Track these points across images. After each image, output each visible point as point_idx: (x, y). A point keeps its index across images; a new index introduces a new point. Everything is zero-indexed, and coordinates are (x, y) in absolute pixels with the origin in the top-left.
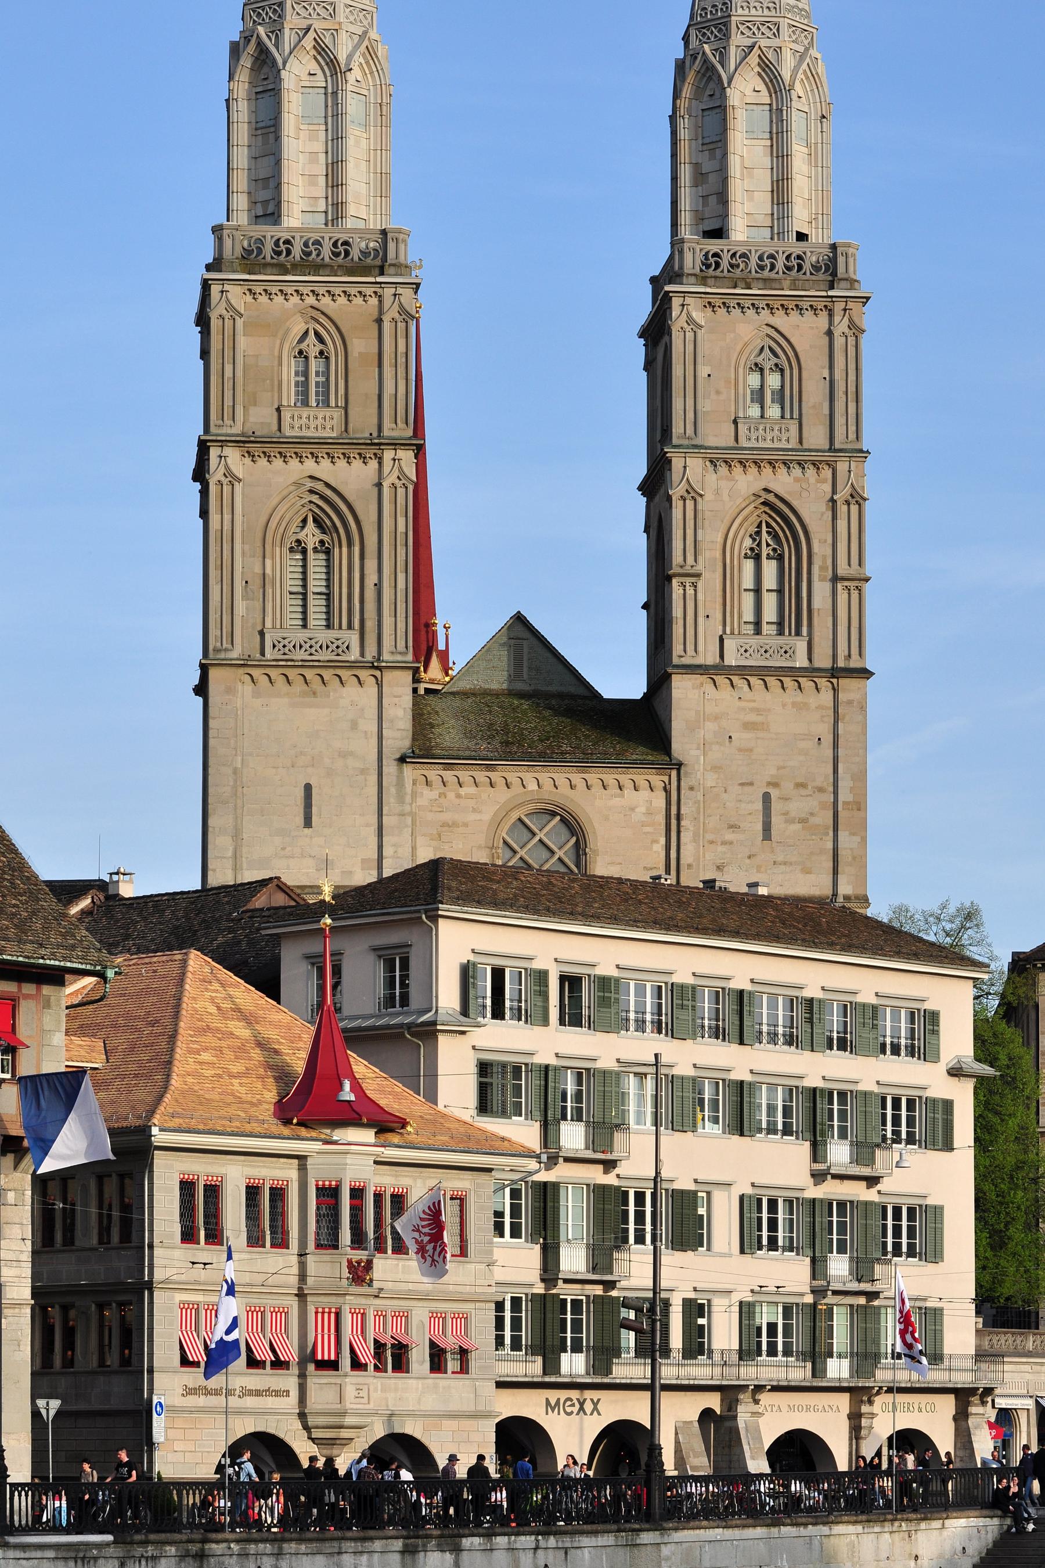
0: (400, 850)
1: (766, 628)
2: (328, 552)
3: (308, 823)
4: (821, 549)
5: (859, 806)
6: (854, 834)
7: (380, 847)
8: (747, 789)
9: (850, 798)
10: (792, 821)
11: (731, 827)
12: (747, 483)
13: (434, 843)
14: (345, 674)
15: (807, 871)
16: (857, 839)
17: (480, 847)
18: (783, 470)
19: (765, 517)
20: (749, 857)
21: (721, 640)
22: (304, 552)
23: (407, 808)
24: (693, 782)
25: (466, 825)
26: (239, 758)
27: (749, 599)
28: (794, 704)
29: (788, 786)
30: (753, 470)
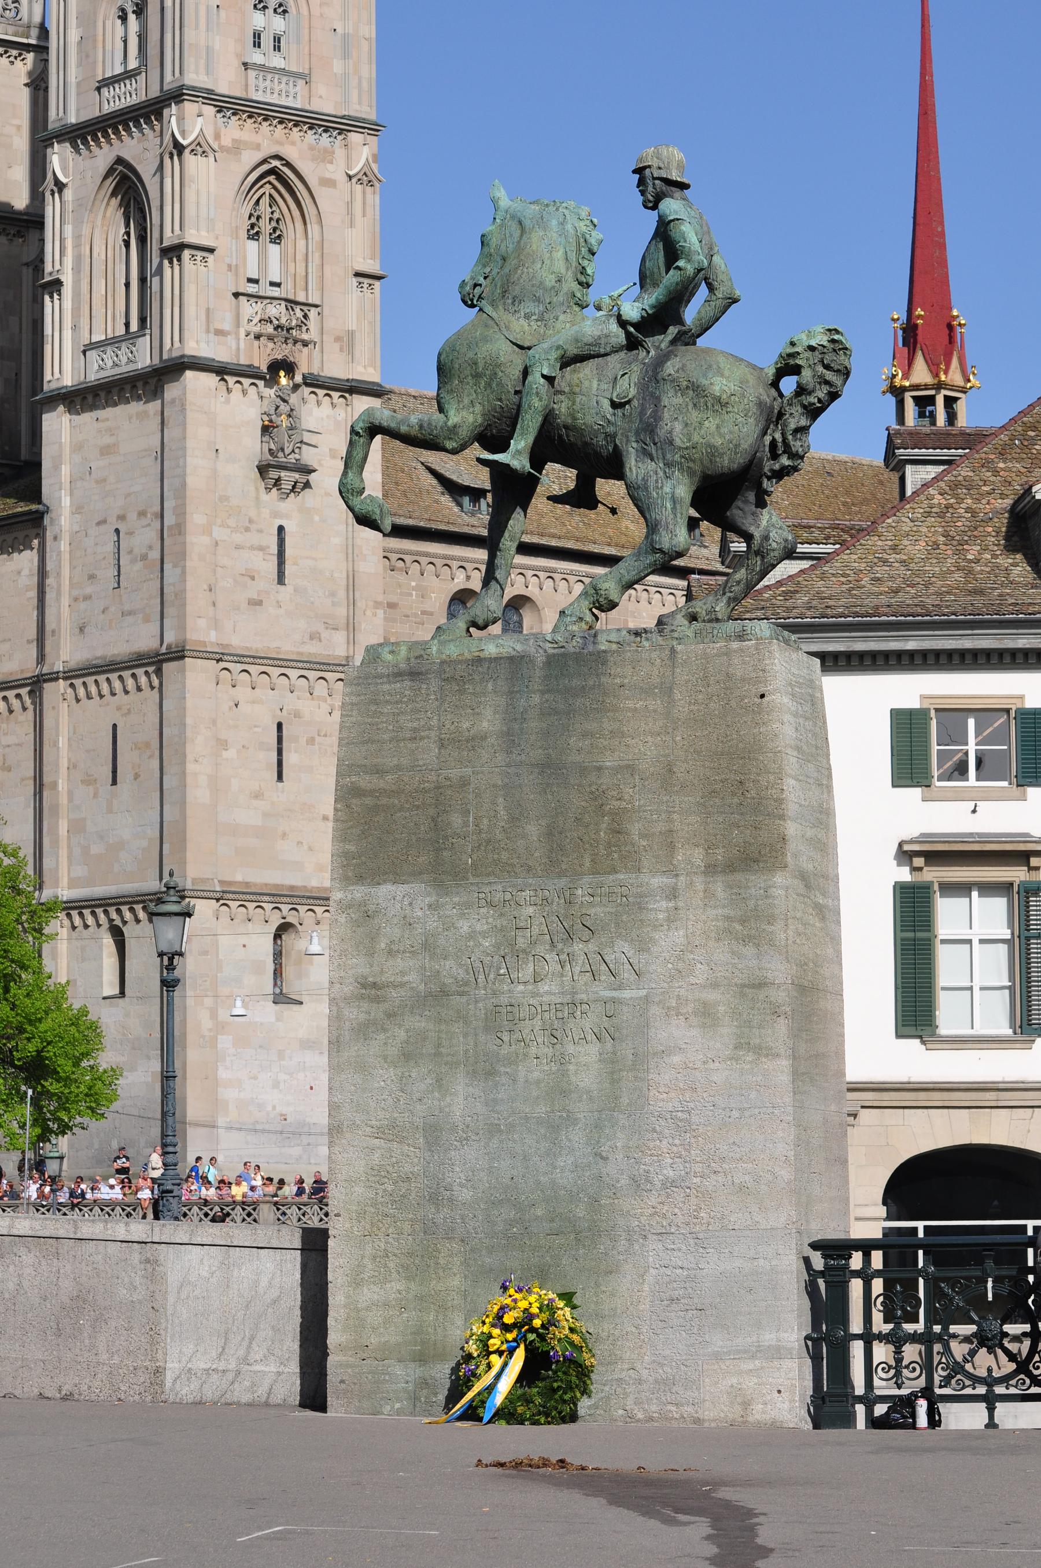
5: (180, 529)
6: (175, 566)
8: (103, 528)
9: (173, 522)
11: (92, 577)
12: (103, 156)
16: (178, 571)
29: (132, 516)
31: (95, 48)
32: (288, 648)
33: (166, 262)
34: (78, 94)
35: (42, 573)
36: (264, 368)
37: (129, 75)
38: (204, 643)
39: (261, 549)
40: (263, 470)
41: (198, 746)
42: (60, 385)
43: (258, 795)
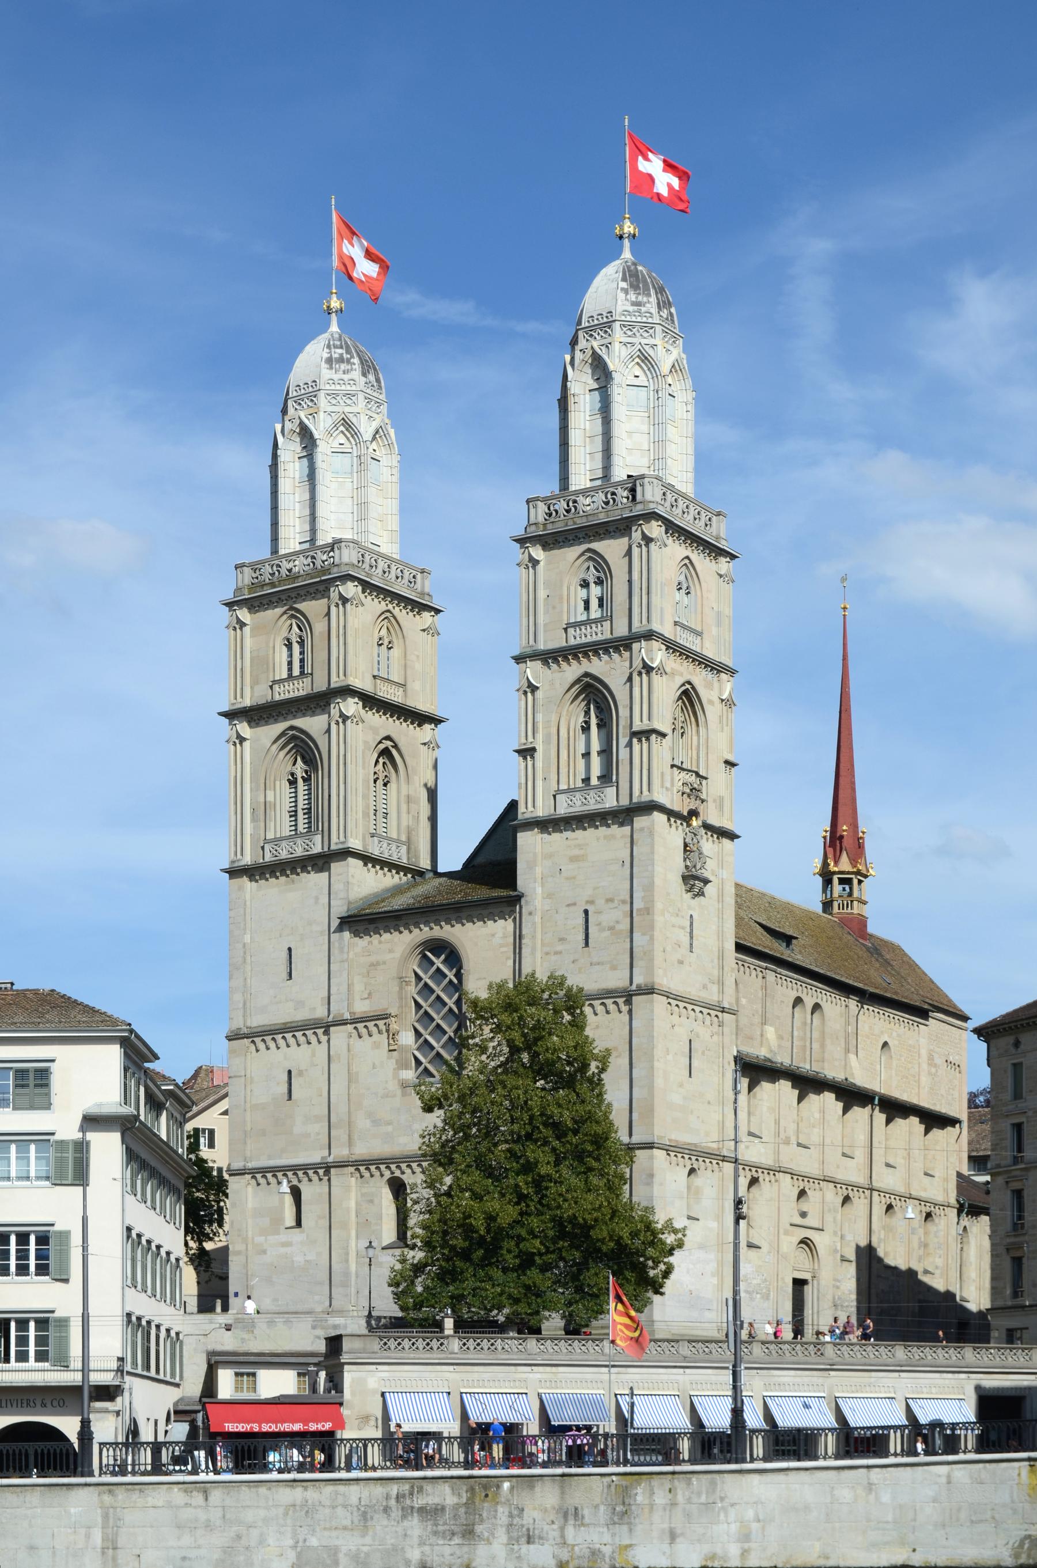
1: (594, 781)
4: (624, 712)
5: (648, 911)
6: (644, 934)
8: (572, 908)
10: (604, 930)
15: (614, 968)
16: (647, 938)
18: (594, 659)
19: (591, 695)
21: (554, 796)
24: (531, 908)
27: (581, 763)
28: (605, 837)
29: (600, 902)
30: (574, 662)
31: (562, 602)
32: (694, 993)
33: (635, 740)
34: (545, 631)
35: (518, 938)
36: (685, 814)
37: (588, 622)
38: (660, 985)
39: (683, 928)
40: (685, 878)
41: (658, 1052)
42: (534, 815)
43: (681, 1085)
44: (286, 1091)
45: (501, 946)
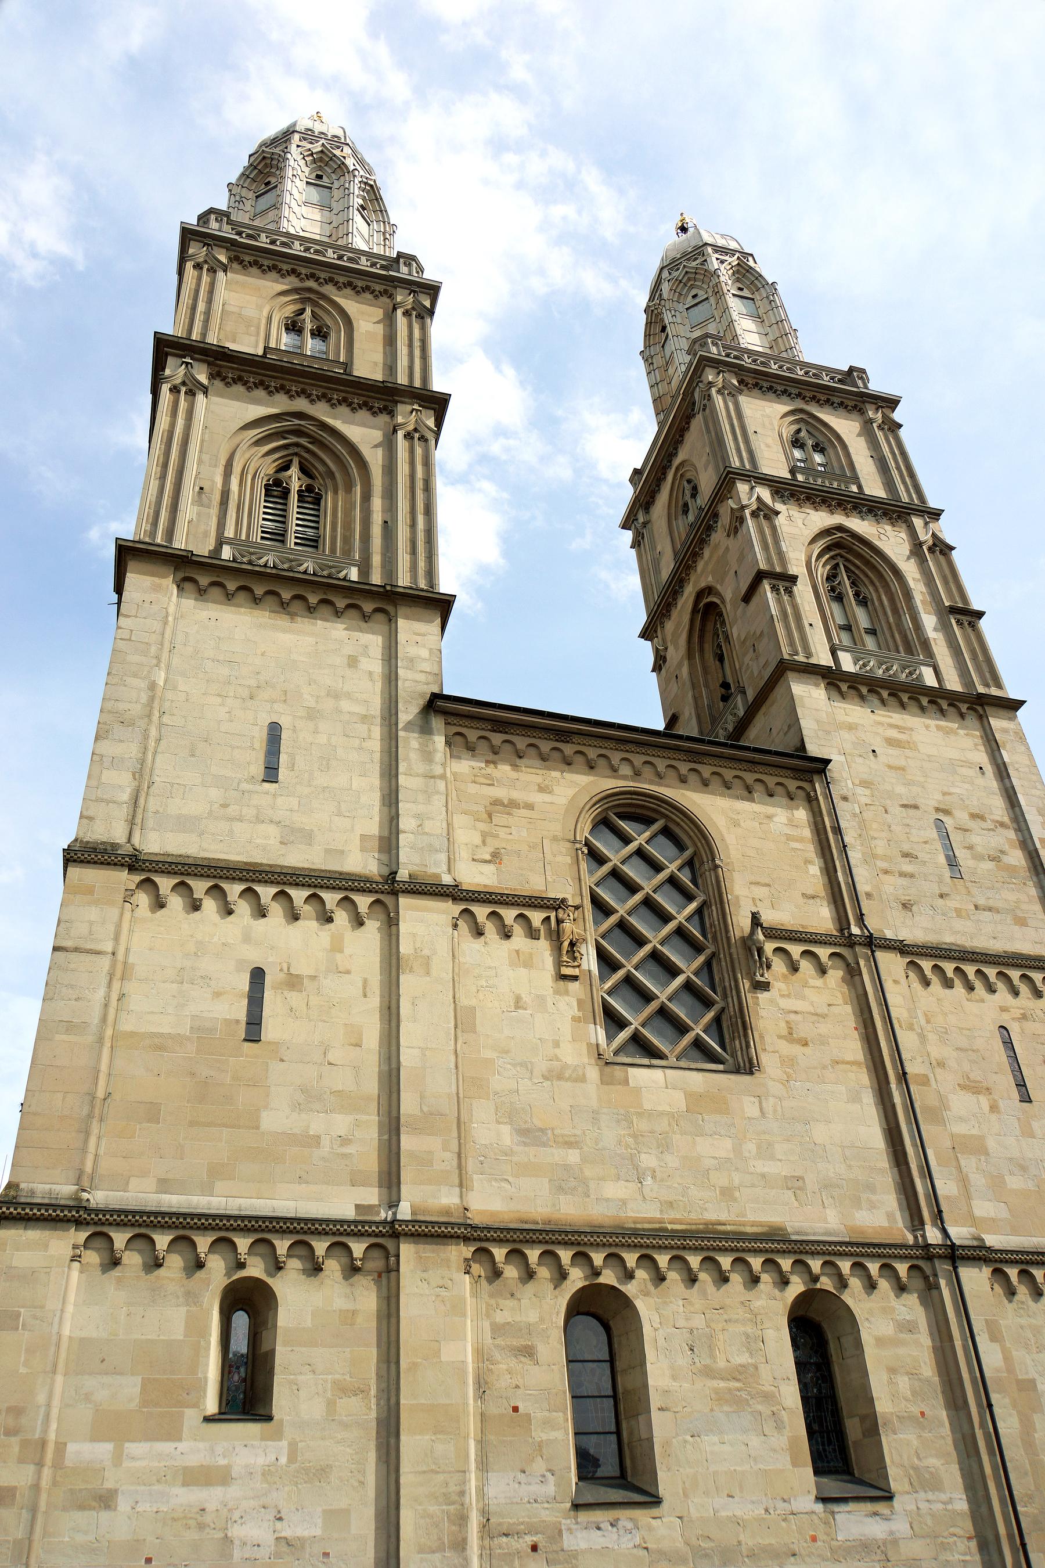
0: (428, 826)
2: (317, 501)
3: (271, 773)
7: (392, 821)
8: (912, 812)
11: (906, 855)
13: (481, 826)
14: (341, 603)
17: (555, 839)
20: (941, 896)
22: (285, 494)
23: (438, 770)
24: (844, 792)
25: (530, 807)
26: (163, 674)
29: (962, 816)
44: (242, 1015)
45: (789, 838)
